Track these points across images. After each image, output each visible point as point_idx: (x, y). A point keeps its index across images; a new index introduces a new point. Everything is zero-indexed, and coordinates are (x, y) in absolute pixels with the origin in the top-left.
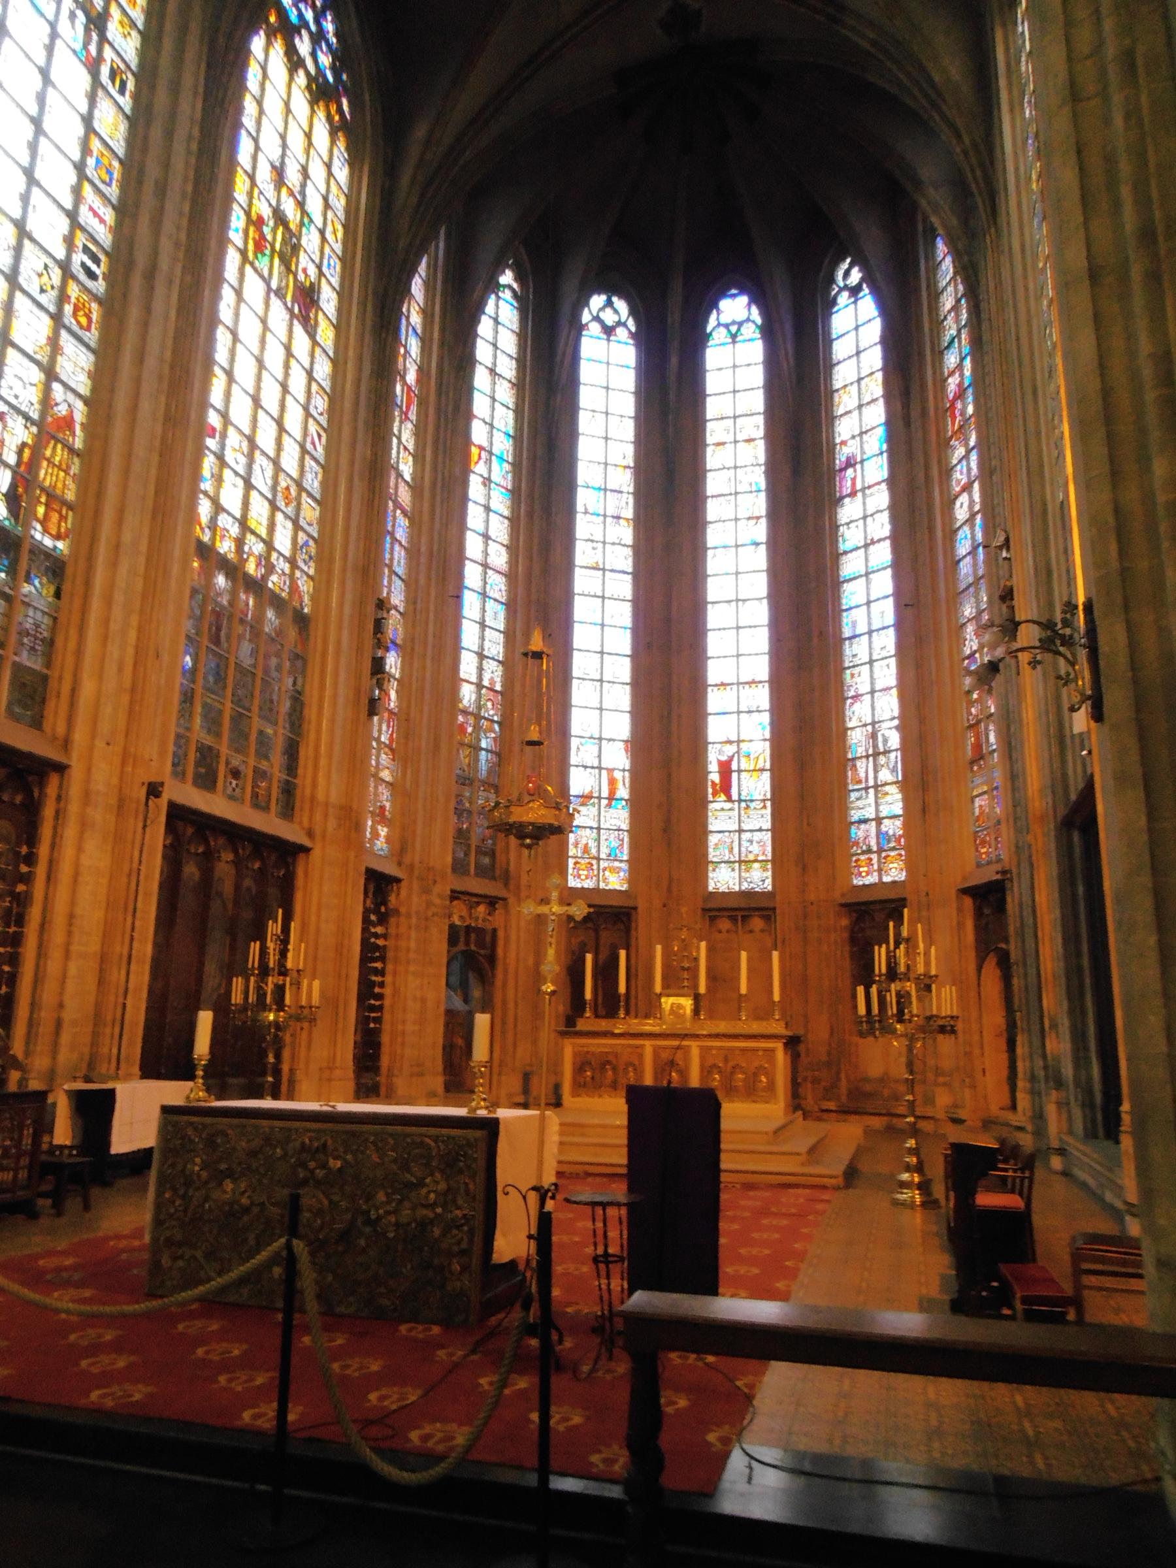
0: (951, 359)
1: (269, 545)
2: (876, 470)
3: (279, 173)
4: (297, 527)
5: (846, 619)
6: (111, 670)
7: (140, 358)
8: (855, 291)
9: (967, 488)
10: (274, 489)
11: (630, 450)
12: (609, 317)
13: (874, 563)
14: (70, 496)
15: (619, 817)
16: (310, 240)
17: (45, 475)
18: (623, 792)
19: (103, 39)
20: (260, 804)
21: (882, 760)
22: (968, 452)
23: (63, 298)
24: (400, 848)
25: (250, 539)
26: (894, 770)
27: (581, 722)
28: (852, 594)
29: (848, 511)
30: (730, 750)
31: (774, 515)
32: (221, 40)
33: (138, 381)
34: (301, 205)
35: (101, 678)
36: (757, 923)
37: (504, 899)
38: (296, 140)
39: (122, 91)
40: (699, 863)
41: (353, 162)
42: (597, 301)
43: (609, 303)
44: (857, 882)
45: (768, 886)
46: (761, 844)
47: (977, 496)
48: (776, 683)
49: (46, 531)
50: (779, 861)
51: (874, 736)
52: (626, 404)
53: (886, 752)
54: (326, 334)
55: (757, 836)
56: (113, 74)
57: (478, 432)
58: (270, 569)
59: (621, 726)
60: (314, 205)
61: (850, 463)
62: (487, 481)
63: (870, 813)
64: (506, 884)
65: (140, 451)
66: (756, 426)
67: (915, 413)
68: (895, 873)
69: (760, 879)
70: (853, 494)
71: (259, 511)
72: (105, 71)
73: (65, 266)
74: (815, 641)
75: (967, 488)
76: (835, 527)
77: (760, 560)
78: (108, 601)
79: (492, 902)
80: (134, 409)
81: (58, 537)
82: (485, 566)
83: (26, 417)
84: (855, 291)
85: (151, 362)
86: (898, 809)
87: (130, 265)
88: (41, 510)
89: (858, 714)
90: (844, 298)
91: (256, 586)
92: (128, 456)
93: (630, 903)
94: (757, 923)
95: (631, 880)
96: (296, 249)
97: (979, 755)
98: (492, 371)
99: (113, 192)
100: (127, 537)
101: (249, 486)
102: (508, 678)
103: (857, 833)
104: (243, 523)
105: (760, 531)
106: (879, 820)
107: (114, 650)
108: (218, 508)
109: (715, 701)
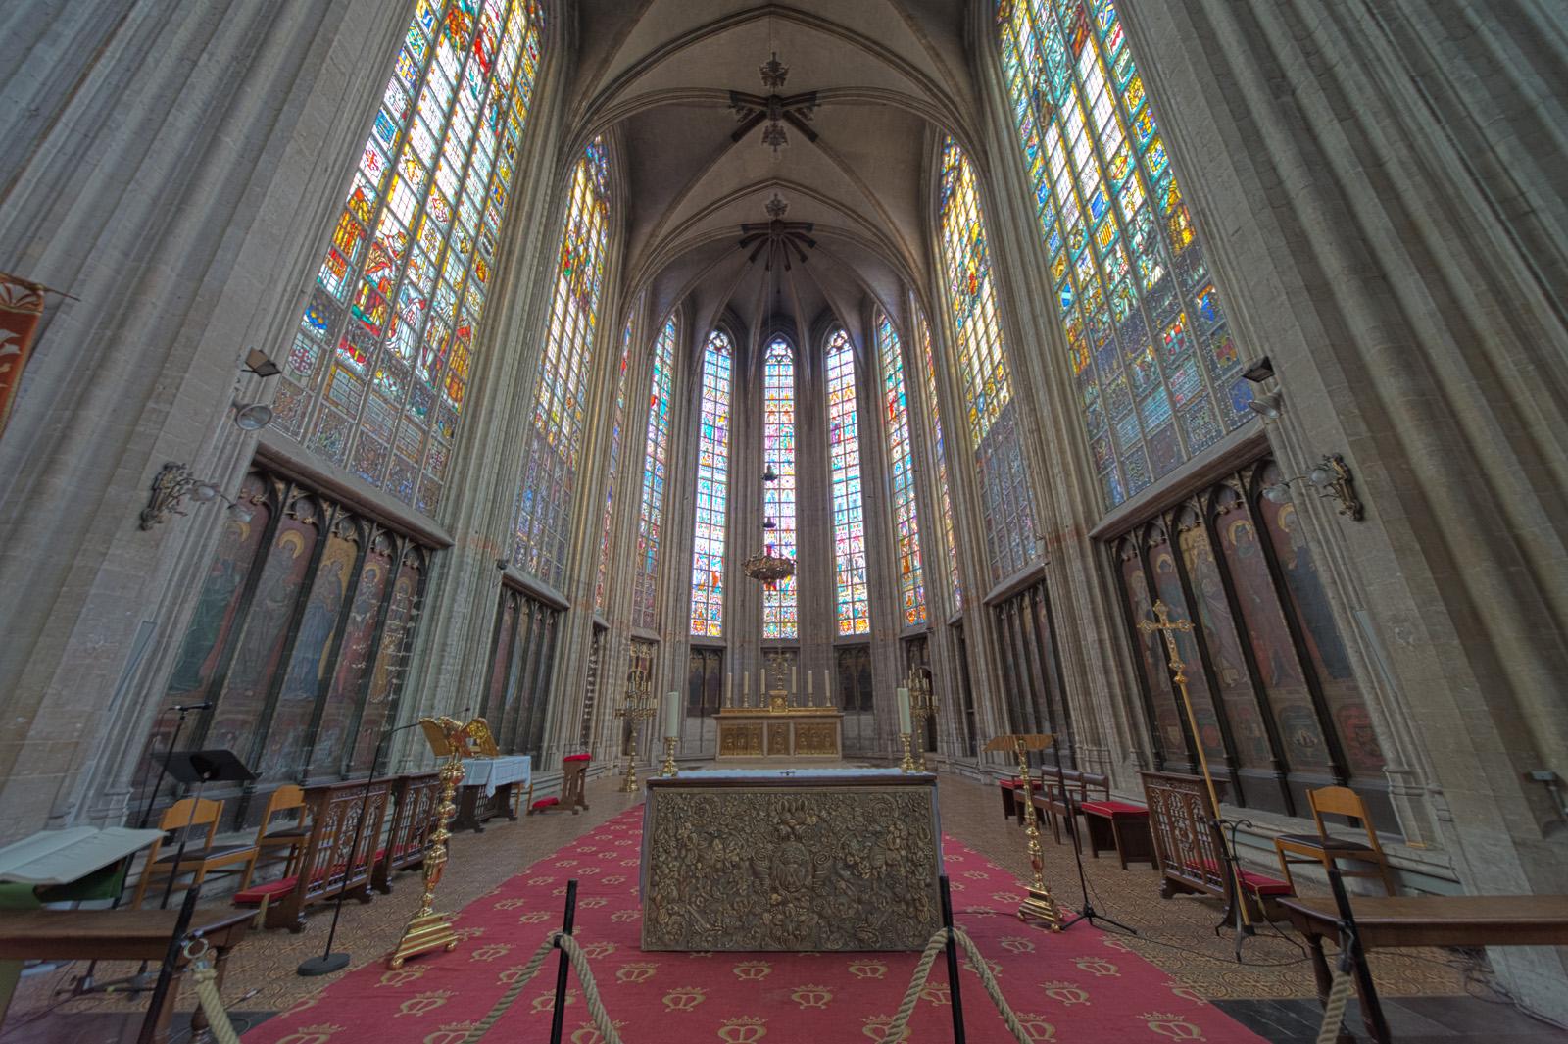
0: (890, 385)
1: (560, 428)
2: (852, 432)
3: (578, 229)
4: (573, 423)
5: (836, 502)
6: (483, 486)
7: (512, 307)
8: (839, 349)
9: (900, 443)
10: (564, 396)
11: (727, 409)
12: (718, 343)
13: (850, 475)
14: (465, 377)
15: (717, 597)
16: (589, 270)
17: (453, 361)
18: (720, 584)
19: (504, 127)
20: (545, 577)
22: (901, 427)
23: (471, 260)
24: (608, 612)
25: (552, 423)
26: (861, 578)
27: (700, 544)
28: (838, 490)
29: (836, 450)
31: (798, 449)
32: (566, 149)
33: (509, 318)
34: (586, 249)
35: (476, 490)
38: (586, 217)
39: (512, 157)
40: (759, 623)
41: (608, 236)
42: (714, 335)
43: (718, 336)
44: (842, 634)
45: (795, 635)
46: (792, 614)
47: (907, 449)
48: (800, 531)
49: (449, 394)
50: (802, 622)
51: (850, 560)
52: (724, 386)
53: (857, 568)
54: (592, 320)
56: (508, 146)
57: (655, 390)
58: (560, 442)
59: (718, 548)
60: (592, 252)
61: (837, 427)
62: (657, 415)
63: (849, 599)
65: (508, 358)
66: (789, 406)
67: (872, 407)
68: (863, 628)
69: (791, 632)
70: (839, 442)
71: (556, 407)
72: (504, 142)
73: (475, 241)
75: (900, 443)
76: (830, 457)
78: (484, 445)
79: (651, 643)
80: (506, 334)
81: (455, 400)
82: (655, 459)
83: (446, 324)
84: (839, 349)
85: (518, 308)
86: (865, 596)
87: (510, 253)
88: (448, 381)
89: (841, 549)
90: (834, 351)
91: (553, 451)
92: (502, 359)
95: (724, 632)
96: (583, 271)
97: (908, 570)
98: (662, 359)
99: (502, 208)
100: (498, 408)
101: (553, 394)
102: (665, 520)
103: (843, 609)
104: (549, 412)
105: (792, 456)
106: (853, 602)
107: (485, 473)
108: (538, 403)
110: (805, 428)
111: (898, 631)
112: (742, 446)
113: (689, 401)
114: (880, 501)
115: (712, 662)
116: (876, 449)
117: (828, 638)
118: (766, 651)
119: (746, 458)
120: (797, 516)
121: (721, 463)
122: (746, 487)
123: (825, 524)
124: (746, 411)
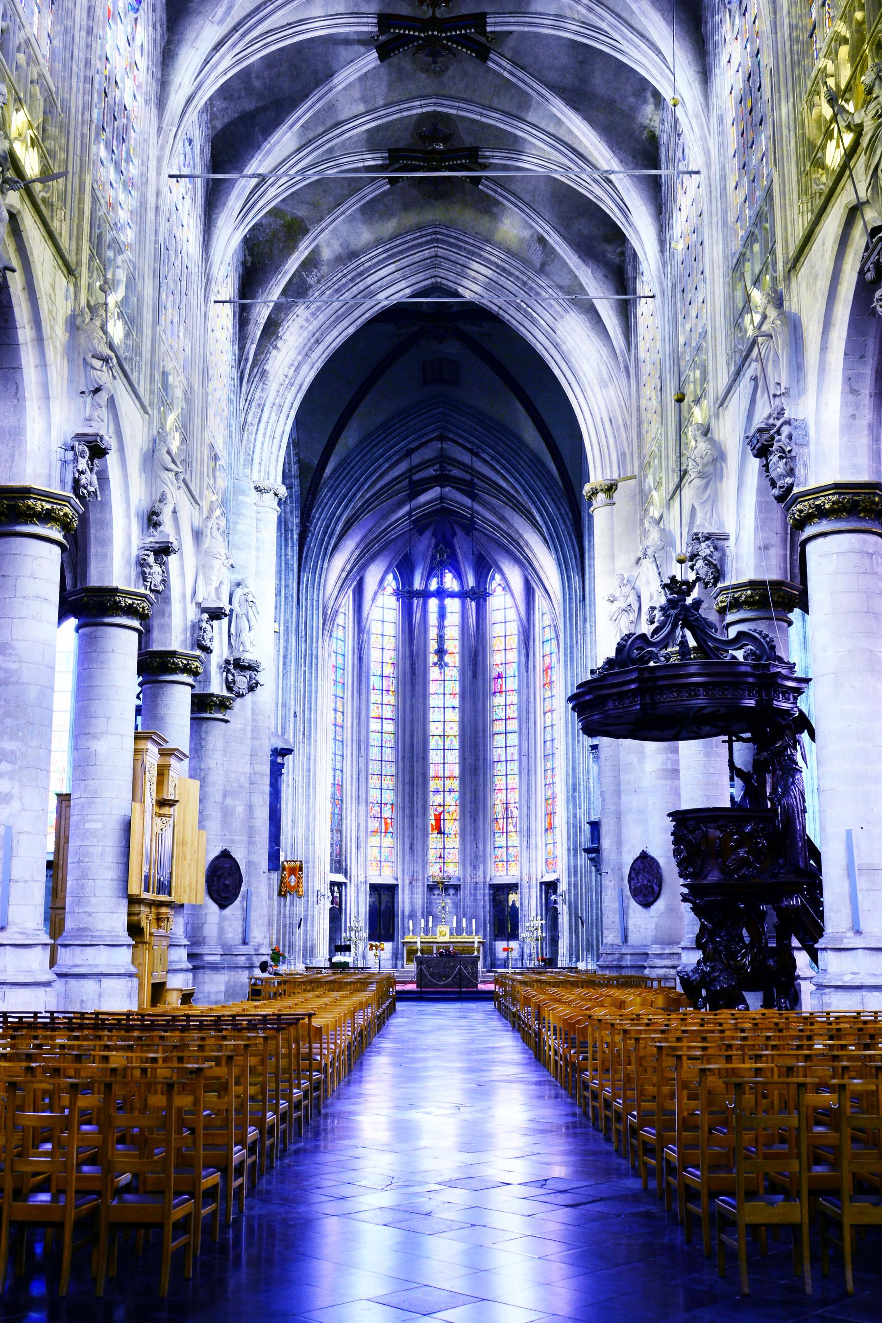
2: (512, 684)
21: (510, 821)
30: (440, 809)
31: (463, 696)
36: (452, 892)
37: (345, 884)
48: (462, 778)
51: (507, 809)
55: (452, 851)
64: (346, 877)
70: (501, 692)
74: (481, 762)
77: (454, 716)
93: (395, 882)
94: (452, 892)
105: (456, 702)
109: (433, 785)
110: (469, 674)
111: (539, 876)
112: (408, 694)
113: (360, 659)
114: (532, 760)
115: (385, 898)
116: (532, 710)
117: (485, 877)
118: (431, 888)
119: (412, 706)
120: (459, 763)
121: (388, 712)
122: (412, 736)
123: (485, 774)
124: (412, 656)
